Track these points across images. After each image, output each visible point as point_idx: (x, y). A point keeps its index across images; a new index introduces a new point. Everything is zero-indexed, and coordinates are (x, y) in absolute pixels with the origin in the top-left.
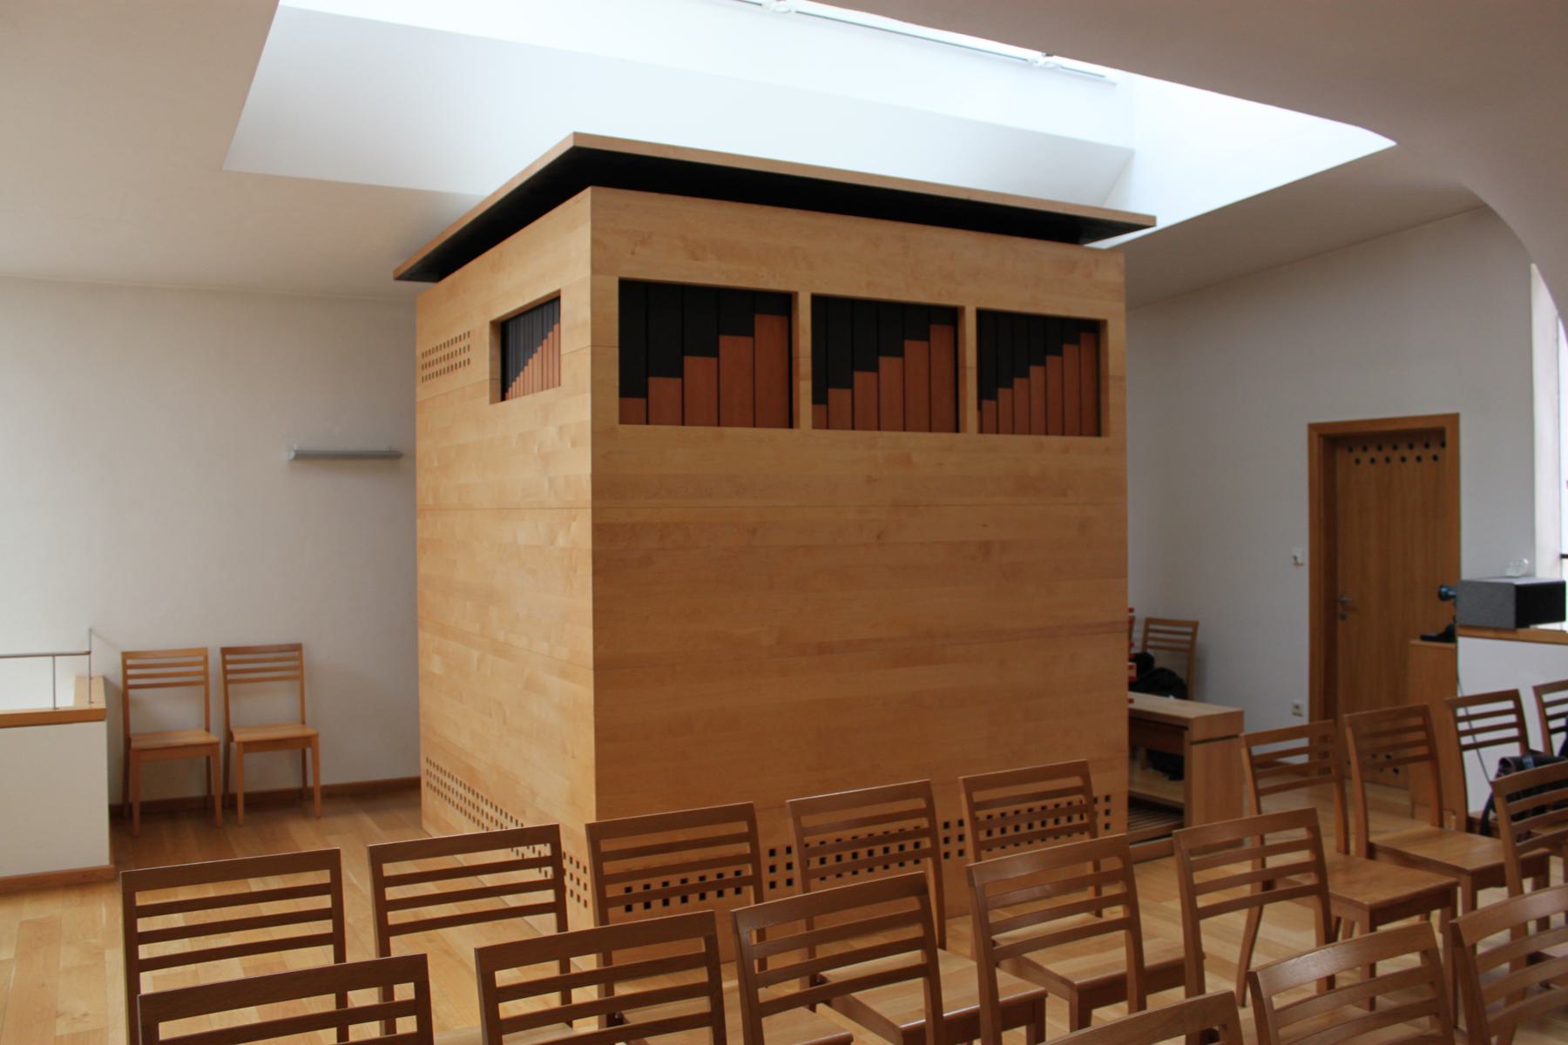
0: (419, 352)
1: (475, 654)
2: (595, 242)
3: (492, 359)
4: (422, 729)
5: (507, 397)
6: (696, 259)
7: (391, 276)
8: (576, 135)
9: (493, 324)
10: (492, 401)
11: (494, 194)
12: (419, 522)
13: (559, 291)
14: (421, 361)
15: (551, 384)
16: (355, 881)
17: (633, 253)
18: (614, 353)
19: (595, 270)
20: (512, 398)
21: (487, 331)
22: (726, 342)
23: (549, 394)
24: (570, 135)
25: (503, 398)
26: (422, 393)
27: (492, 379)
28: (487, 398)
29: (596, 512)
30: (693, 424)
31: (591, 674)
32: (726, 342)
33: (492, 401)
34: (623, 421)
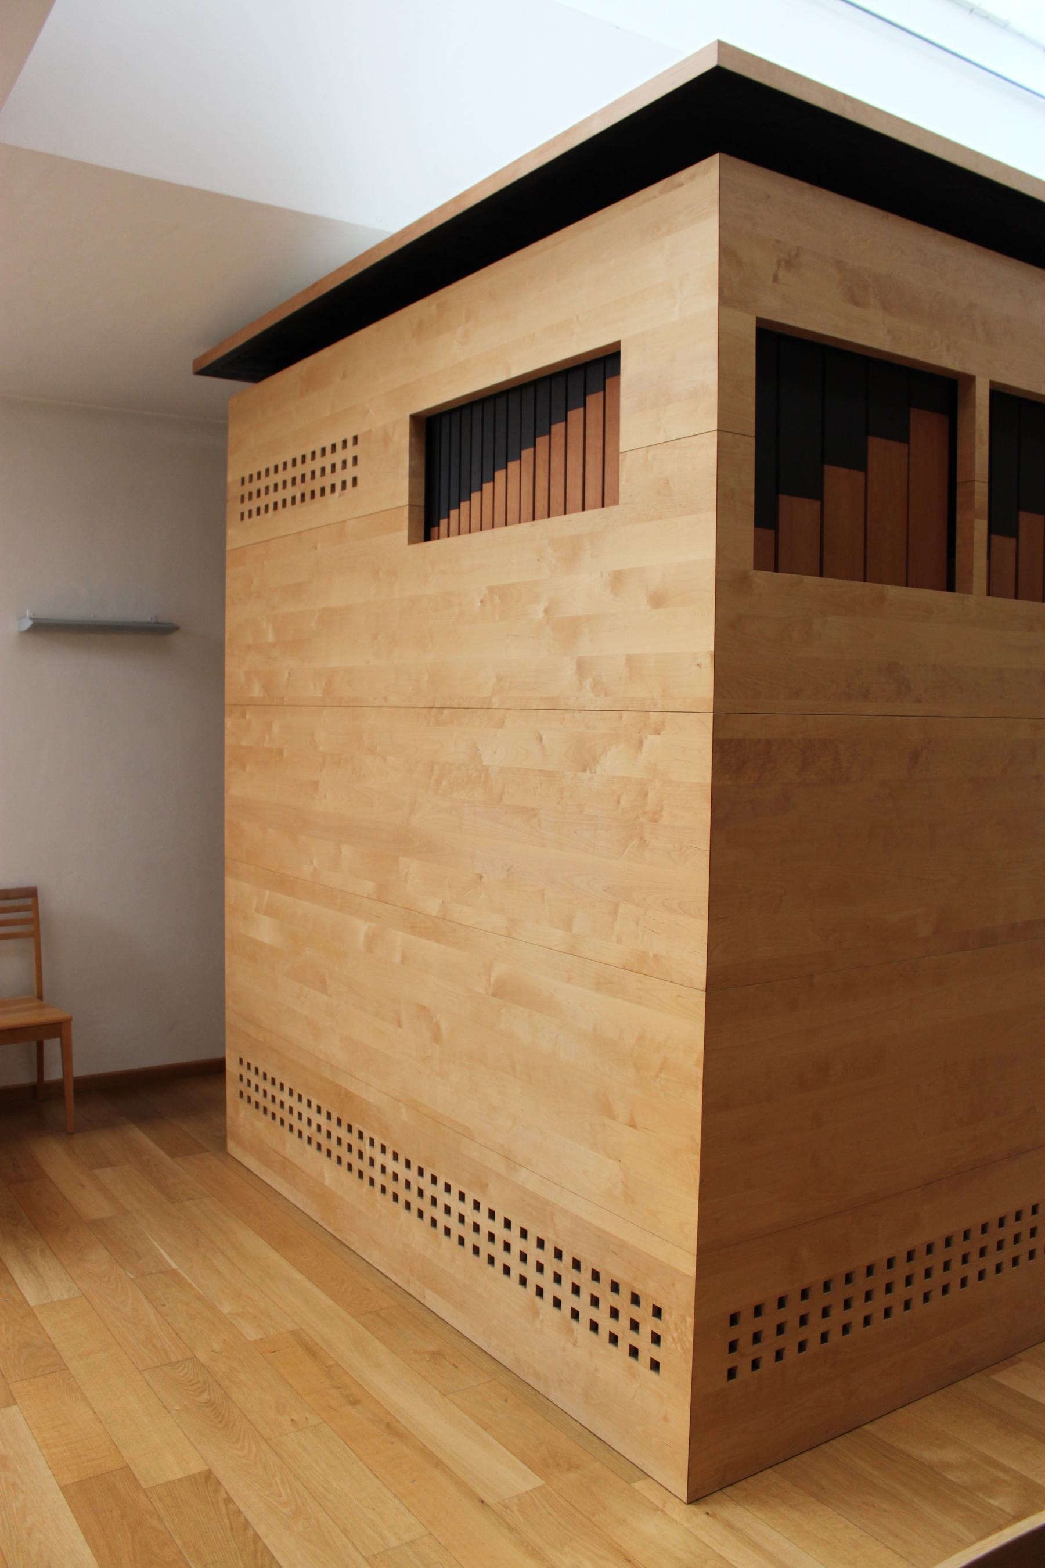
0: (233, 476)
1: (362, 928)
2: (726, 252)
3: (412, 474)
4: (230, 1017)
5: (432, 536)
6: (856, 303)
7: (190, 368)
8: (722, 47)
9: (415, 419)
10: (412, 540)
11: (368, 254)
12: (229, 722)
13: (618, 344)
14: (235, 490)
15: (499, 517)
16: (175, 1266)
17: (775, 279)
18: (747, 448)
19: (725, 300)
20: (434, 539)
21: (402, 439)
22: (876, 446)
23: (593, 517)
24: (714, 43)
25: (427, 538)
26: (236, 536)
27: (411, 506)
28: (404, 533)
29: (720, 718)
30: (833, 575)
31: (701, 998)
32: (876, 446)
33: (412, 540)
34: (757, 567)
